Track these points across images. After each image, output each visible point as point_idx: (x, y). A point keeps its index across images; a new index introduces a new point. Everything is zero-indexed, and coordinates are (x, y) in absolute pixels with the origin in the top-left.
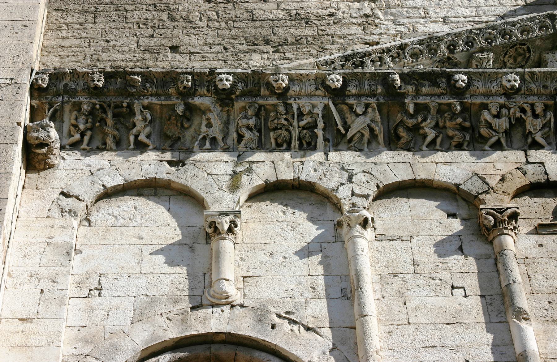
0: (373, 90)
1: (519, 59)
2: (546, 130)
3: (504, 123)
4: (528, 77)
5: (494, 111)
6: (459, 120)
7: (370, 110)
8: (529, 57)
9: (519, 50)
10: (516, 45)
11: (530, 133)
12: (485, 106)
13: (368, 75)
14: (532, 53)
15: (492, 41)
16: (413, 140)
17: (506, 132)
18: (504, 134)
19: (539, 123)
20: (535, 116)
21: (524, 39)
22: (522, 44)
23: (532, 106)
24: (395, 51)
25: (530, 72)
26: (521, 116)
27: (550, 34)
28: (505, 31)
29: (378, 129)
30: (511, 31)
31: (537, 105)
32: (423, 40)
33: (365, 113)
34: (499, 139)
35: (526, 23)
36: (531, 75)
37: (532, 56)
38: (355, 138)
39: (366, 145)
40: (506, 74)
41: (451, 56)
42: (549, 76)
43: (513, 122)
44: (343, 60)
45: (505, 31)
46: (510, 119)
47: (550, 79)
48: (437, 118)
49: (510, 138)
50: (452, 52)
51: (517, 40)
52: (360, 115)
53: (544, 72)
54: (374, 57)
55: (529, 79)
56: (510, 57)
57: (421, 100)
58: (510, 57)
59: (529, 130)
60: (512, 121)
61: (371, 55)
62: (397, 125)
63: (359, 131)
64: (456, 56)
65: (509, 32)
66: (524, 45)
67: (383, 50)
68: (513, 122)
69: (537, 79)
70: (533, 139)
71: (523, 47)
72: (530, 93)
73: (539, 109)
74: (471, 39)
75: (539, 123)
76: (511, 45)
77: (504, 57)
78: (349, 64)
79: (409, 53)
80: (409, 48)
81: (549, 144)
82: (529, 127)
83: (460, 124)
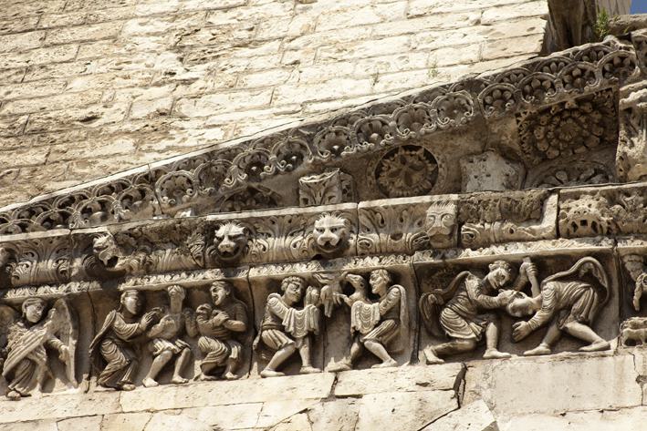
0: (63, 272)
1: (416, 177)
2: (389, 323)
3: (308, 315)
4: (365, 219)
5: (291, 290)
6: (221, 316)
7: (53, 312)
8: (436, 171)
9: (410, 160)
10: (396, 150)
11: (358, 334)
12: (275, 285)
13: (55, 242)
14: (439, 162)
15: (342, 148)
16: (132, 366)
17: (310, 335)
18: (307, 340)
19: (375, 309)
20: (372, 297)
21: (410, 138)
22: (410, 147)
23: (367, 276)
24: (135, 187)
25: (368, 209)
26: (342, 300)
27: (468, 122)
28: (371, 125)
29: (68, 347)
30: (384, 124)
31: (374, 274)
32: (194, 159)
33: (44, 317)
34: (297, 352)
35: (417, 106)
36: (371, 214)
37: (440, 170)
38: (18, 372)
39: (38, 386)
40: (318, 215)
41: (255, 185)
42: (405, 213)
43: (328, 313)
44: (26, 214)
45: (371, 125)
46: (321, 308)
47: (408, 219)
48: (182, 317)
49: (324, 347)
50: (252, 176)
51: (397, 139)
52: (34, 324)
53: (394, 207)
54: (91, 202)
55: (368, 221)
56: (394, 175)
57: (153, 282)
58: (394, 175)
59: (354, 328)
60: (326, 311)
61: (85, 198)
62: (103, 338)
63: (26, 358)
64: (264, 184)
65: (380, 124)
66: (417, 148)
67: (110, 186)
68: (328, 313)
69: (383, 222)
70: (362, 345)
71: (413, 153)
72: (366, 251)
73: (377, 282)
74: (297, 146)
75: (375, 309)
76: (385, 152)
77: (377, 176)
78: (35, 221)
79: (165, 186)
80: (163, 177)
81: (393, 355)
82: (356, 322)
83: (222, 326)
